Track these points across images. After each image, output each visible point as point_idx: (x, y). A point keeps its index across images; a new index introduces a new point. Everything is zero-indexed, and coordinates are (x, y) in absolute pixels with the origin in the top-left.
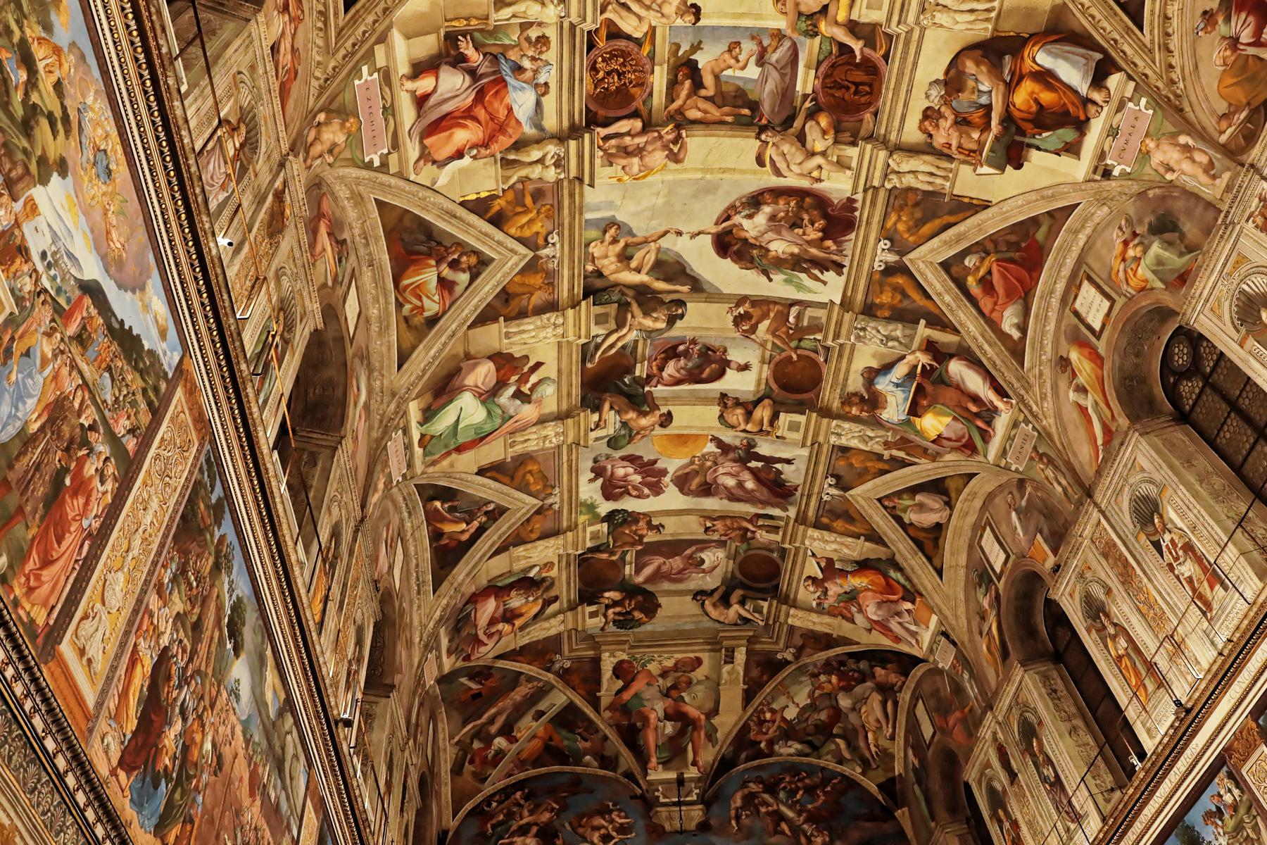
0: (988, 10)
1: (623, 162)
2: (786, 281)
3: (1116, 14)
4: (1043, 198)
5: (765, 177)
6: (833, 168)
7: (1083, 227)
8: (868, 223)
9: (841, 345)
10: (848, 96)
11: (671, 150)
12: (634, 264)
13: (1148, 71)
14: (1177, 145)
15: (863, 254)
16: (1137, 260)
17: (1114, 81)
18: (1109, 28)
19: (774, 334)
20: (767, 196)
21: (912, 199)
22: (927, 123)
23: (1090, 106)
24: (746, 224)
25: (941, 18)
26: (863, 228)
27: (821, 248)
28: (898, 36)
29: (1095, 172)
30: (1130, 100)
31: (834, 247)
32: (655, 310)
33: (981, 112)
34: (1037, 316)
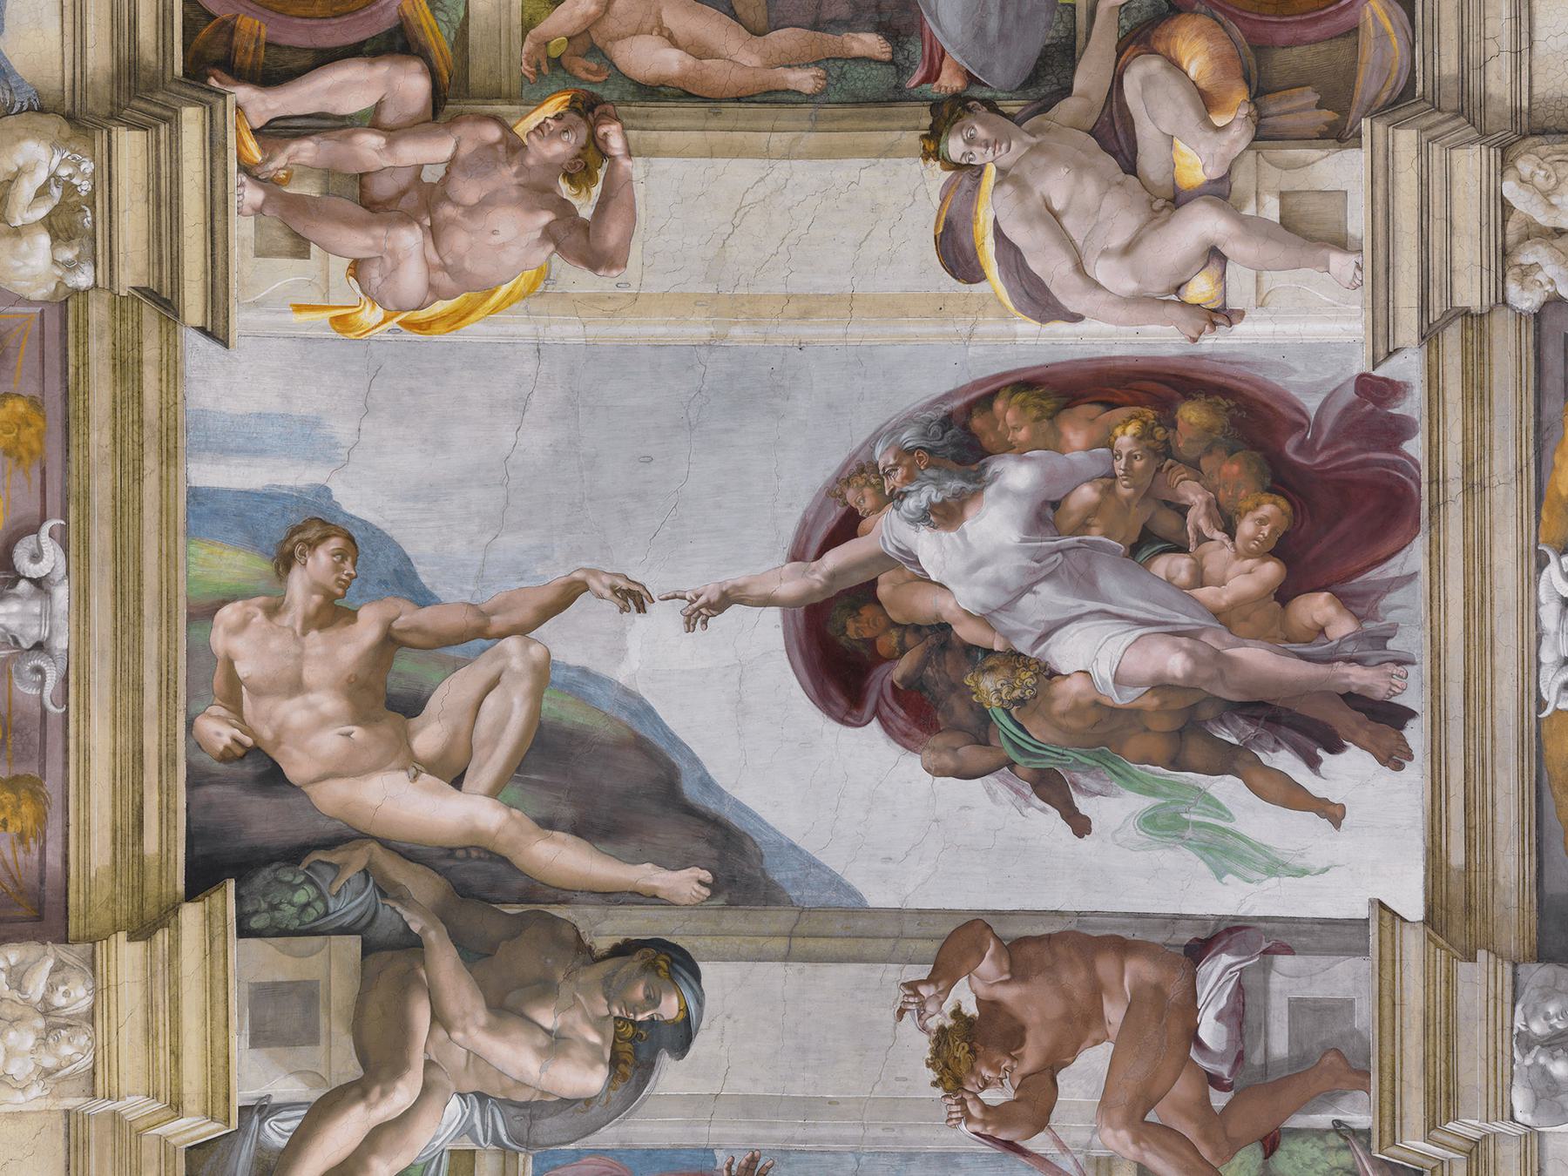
1: (358, 242)
2: (1150, 822)
5: (989, 326)
6: (1273, 252)
8: (1474, 487)
9: (1475, 1150)
11: (564, 209)
12: (428, 737)
15: (1479, 642)
19: (1142, 1129)
20: (1007, 412)
24: (931, 548)
26: (1454, 513)
27: (1284, 637)
31: (1342, 627)
32: (545, 989)
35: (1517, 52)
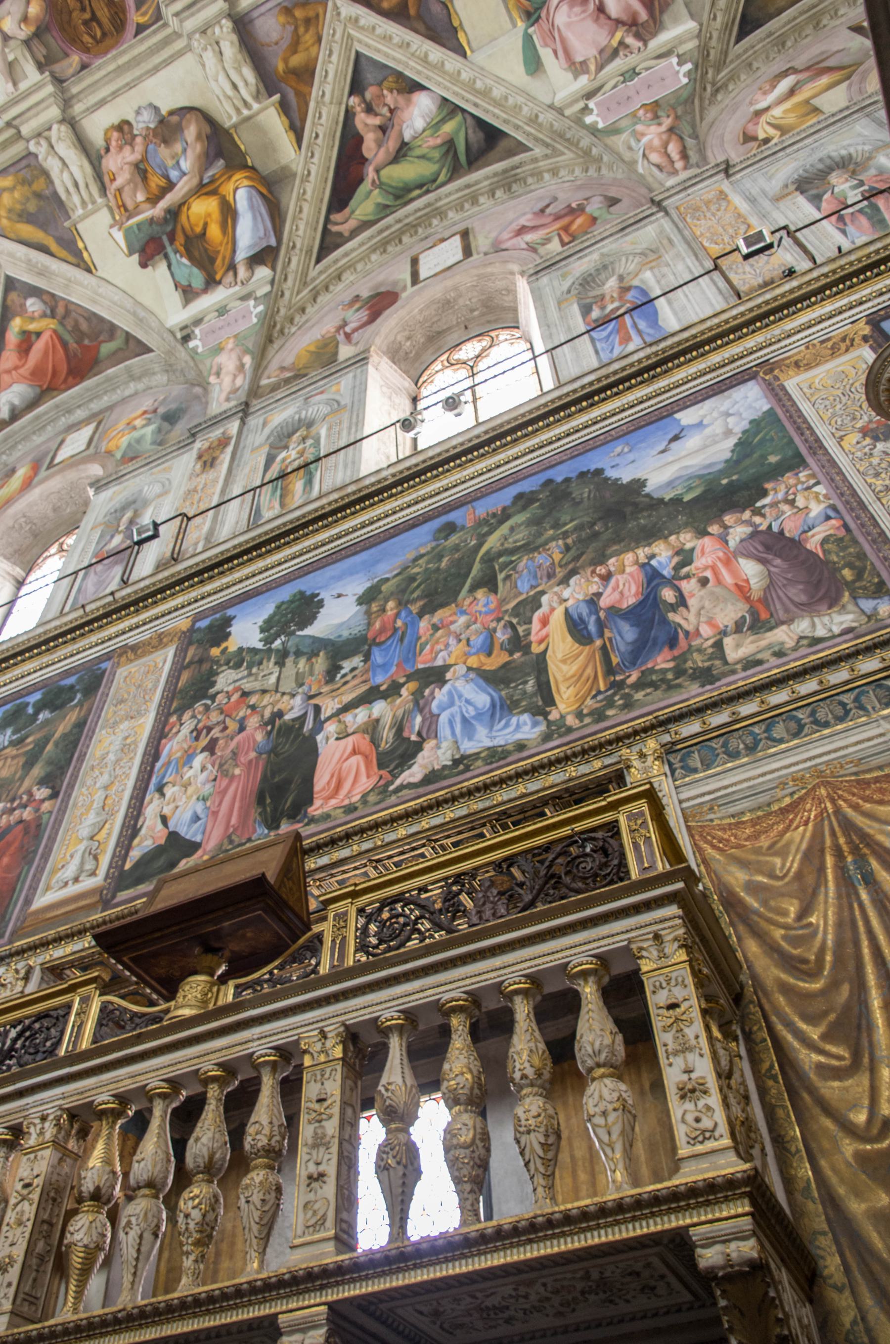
0: (245, 103)
3: (316, 229)
4: (134, 314)
7: (140, 378)
10: (78, 17)
13: (287, 294)
14: (240, 360)
16: (135, 428)
17: (263, 272)
18: (301, 233)
21: (40, 185)
22: (115, 135)
23: (231, 273)
25: (209, 57)
28: (166, 25)
29: (182, 329)
30: (256, 299)
33: (162, 183)
34: (37, 418)
35: (88, 109)
